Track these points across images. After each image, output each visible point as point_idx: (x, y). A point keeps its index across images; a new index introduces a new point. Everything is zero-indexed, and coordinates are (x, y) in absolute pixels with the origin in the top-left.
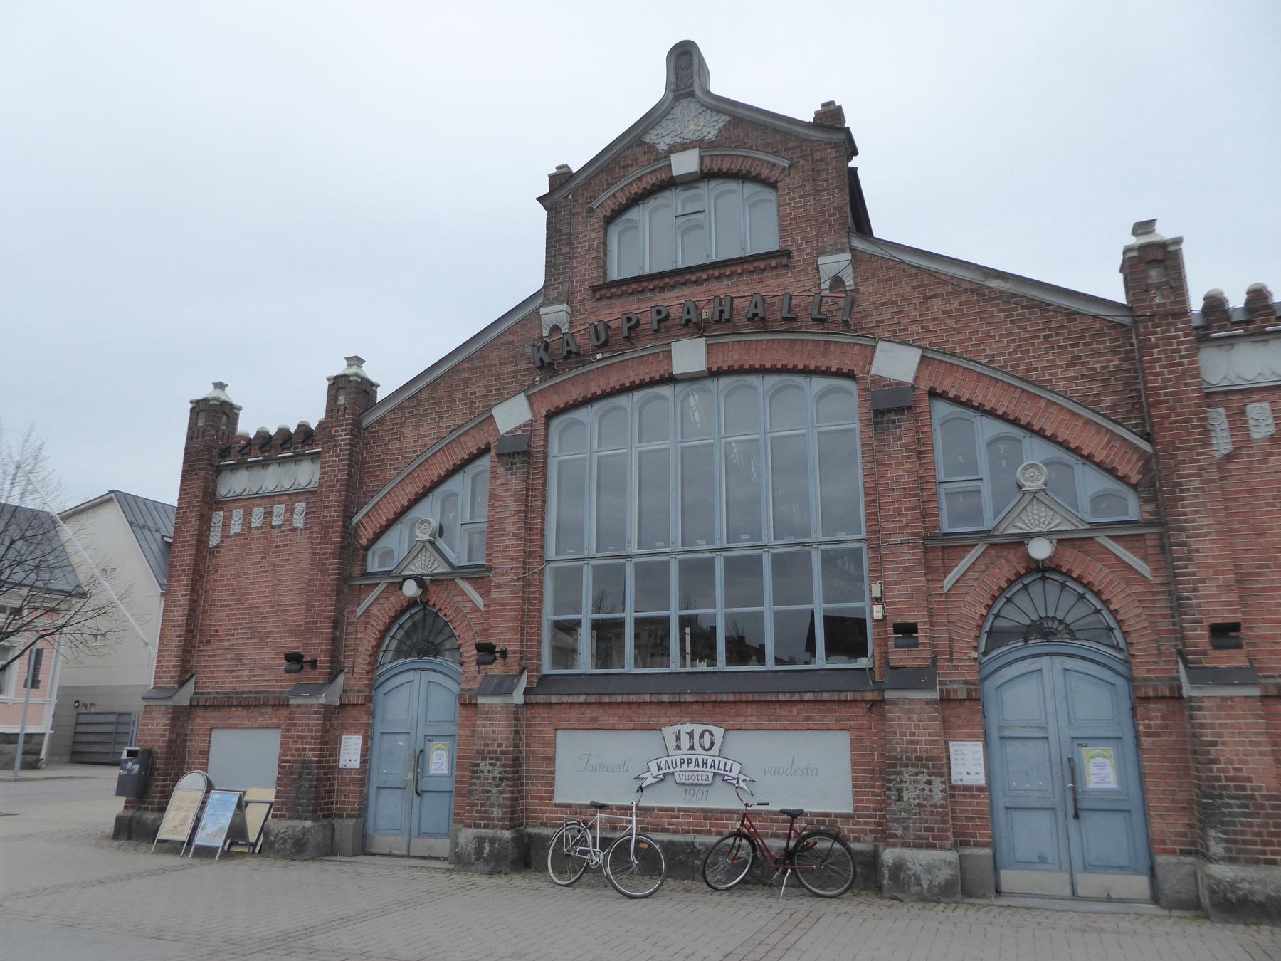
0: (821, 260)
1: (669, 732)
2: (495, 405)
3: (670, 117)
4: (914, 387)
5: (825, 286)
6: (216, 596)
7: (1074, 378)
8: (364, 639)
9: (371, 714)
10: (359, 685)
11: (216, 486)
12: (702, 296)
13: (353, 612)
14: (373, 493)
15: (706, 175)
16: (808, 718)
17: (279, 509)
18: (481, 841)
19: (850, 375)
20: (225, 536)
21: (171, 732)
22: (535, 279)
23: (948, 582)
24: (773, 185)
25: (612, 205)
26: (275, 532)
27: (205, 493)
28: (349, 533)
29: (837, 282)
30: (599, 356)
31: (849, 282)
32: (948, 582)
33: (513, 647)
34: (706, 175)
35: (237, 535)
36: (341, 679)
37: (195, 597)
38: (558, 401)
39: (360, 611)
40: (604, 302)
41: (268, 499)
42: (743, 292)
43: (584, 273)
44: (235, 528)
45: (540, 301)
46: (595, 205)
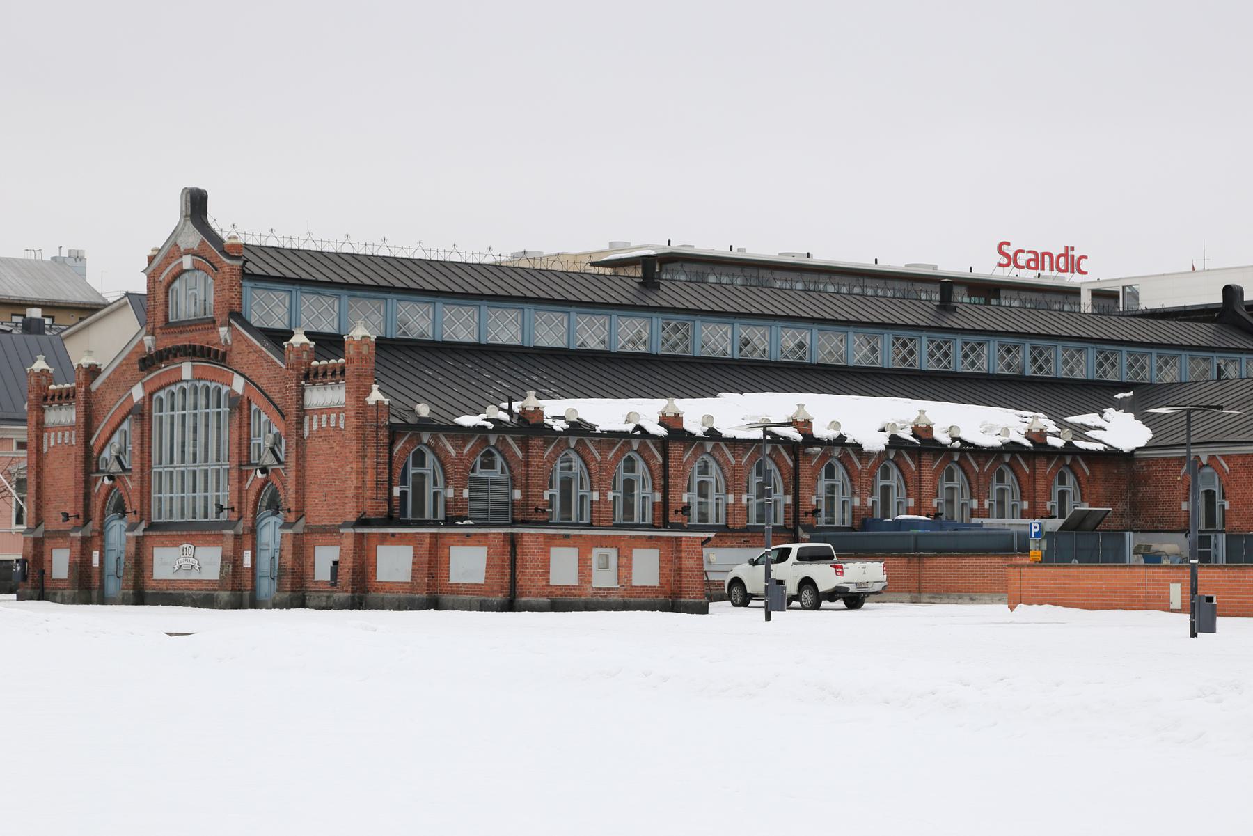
1: (181, 547)
2: (132, 387)
4: (242, 396)
6: (48, 480)
7: (279, 398)
8: (97, 504)
9: (103, 540)
10: (97, 527)
11: (43, 419)
13: (94, 491)
14: (97, 428)
16: (214, 542)
18: (124, 594)
20: (49, 447)
21: (34, 550)
23: (247, 486)
25: (167, 280)
26: (67, 446)
27: (37, 424)
28: (88, 449)
30: (163, 365)
32: (247, 486)
33: (138, 510)
35: (53, 447)
36: (90, 524)
37: (39, 480)
38: (152, 387)
39: (96, 490)
40: (165, 336)
44: (52, 444)
46: (161, 279)
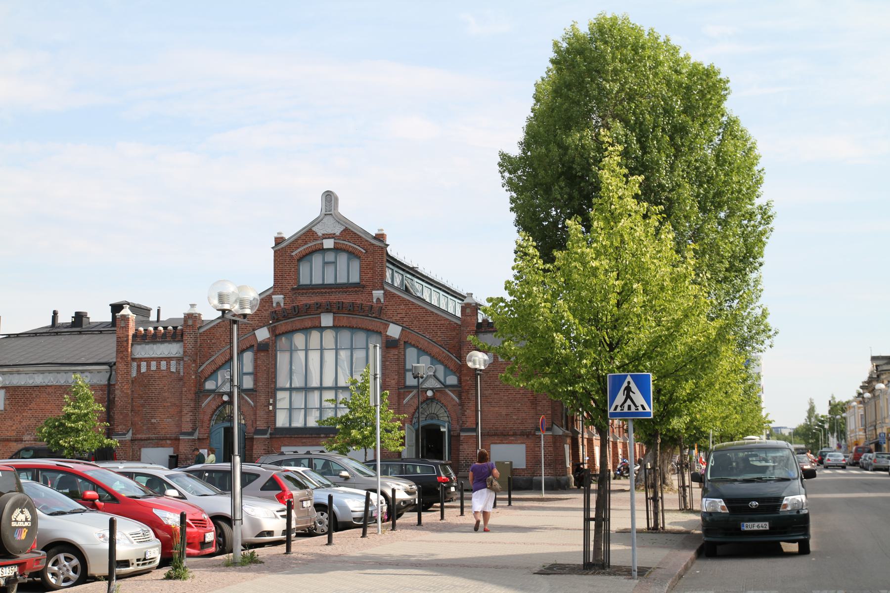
0: (374, 292)
3: (323, 221)
5: (375, 300)
12: (334, 298)
15: (337, 249)
17: (163, 363)
19: (380, 333)
22: (271, 284)
24: (359, 258)
29: (378, 299)
31: (382, 301)
34: (337, 249)
41: (159, 360)
42: (347, 299)
43: (290, 285)
45: (272, 290)
